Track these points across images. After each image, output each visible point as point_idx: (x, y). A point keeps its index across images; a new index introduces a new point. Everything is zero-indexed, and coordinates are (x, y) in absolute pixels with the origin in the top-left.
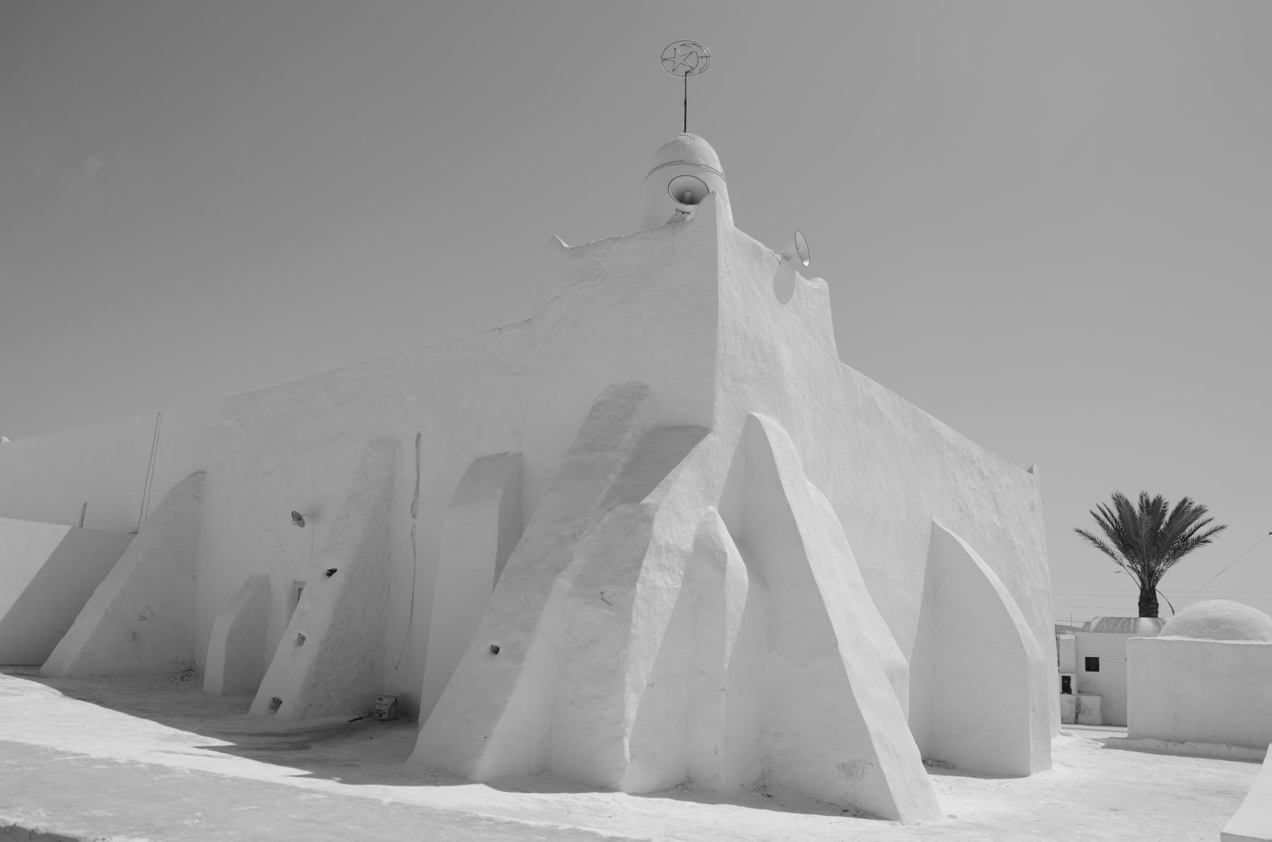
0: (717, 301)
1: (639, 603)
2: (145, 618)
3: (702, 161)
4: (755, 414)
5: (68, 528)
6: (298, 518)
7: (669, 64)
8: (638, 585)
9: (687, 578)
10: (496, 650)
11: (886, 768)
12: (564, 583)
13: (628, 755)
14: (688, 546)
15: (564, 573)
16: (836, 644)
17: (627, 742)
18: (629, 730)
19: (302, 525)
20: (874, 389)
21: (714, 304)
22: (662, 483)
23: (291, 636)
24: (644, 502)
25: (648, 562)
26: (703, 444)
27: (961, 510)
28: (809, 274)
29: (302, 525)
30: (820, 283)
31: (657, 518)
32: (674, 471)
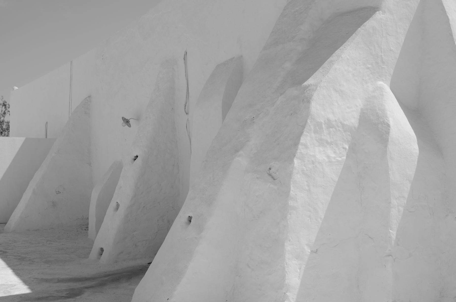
1: (297, 177)
2: (59, 192)
5: (23, 139)
6: (127, 122)
8: (296, 161)
9: (353, 150)
10: (190, 219)
12: (241, 161)
14: (353, 120)
15: (241, 152)
19: (130, 126)
22: (326, 65)
23: (113, 205)
24: (306, 83)
25: (307, 139)
26: (370, 24)
29: (130, 126)
31: (315, 96)
32: (338, 52)
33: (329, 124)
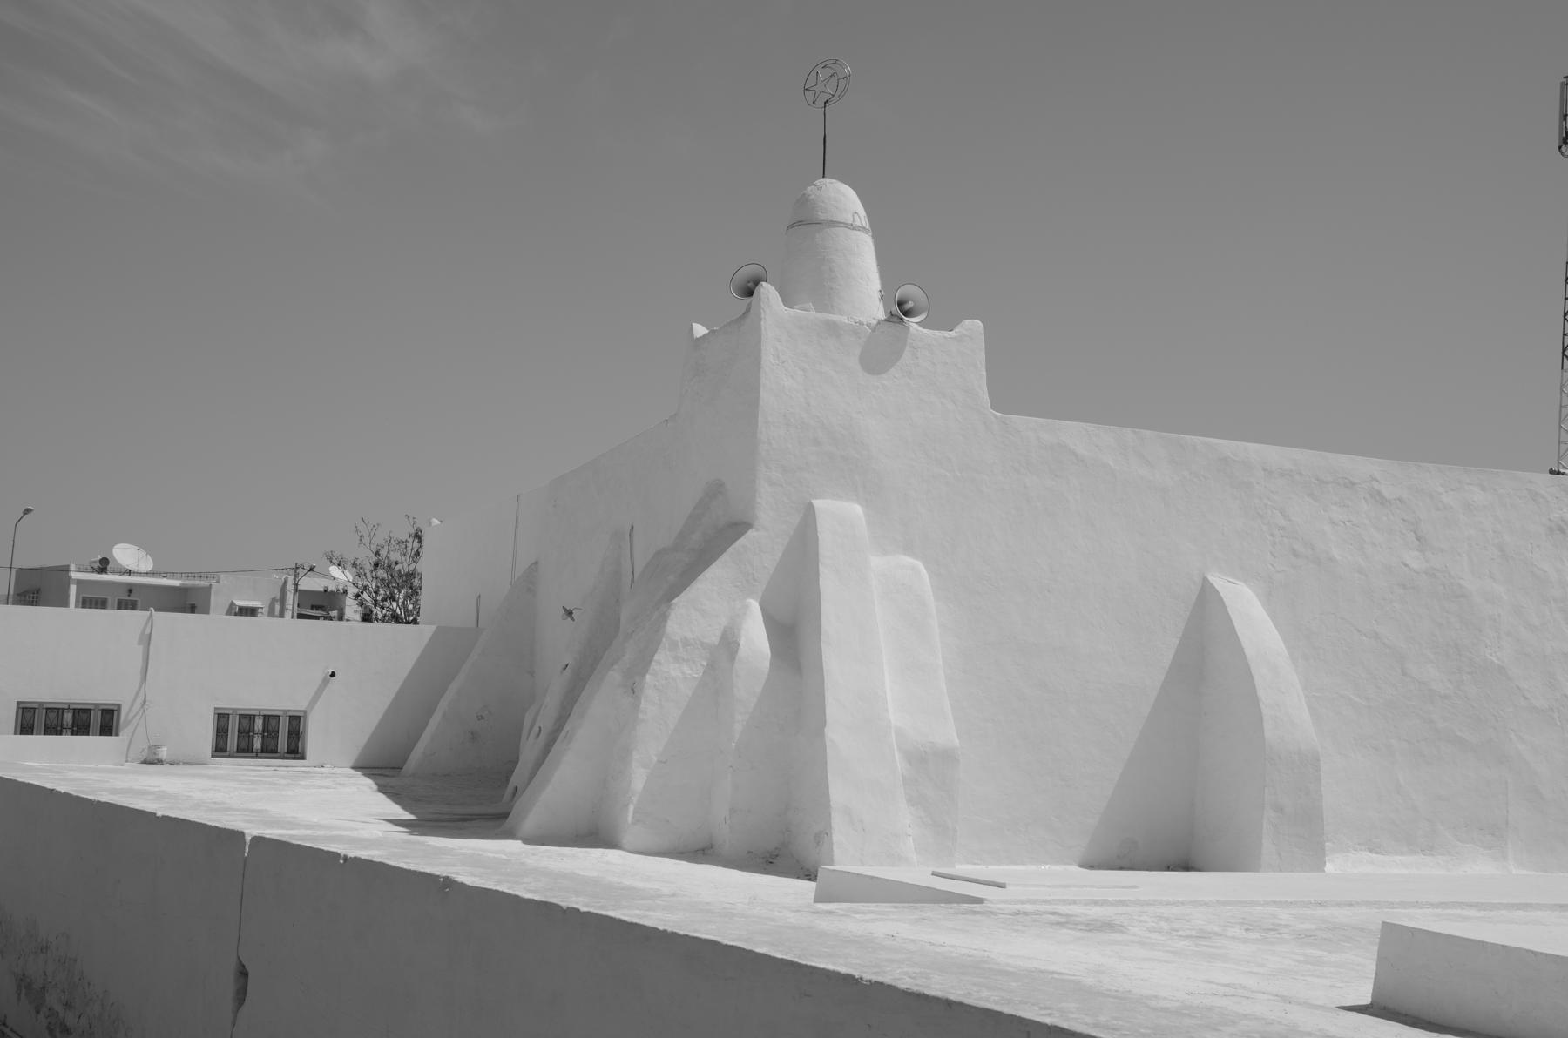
0: (757, 399)
3: (822, 217)
4: (817, 503)
5: (434, 628)
6: (569, 613)
7: (810, 95)
9: (712, 667)
11: (837, 837)
13: (630, 819)
14: (714, 639)
16: (824, 723)
17: (631, 808)
18: (635, 799)
20: (1075, 435)
21: (754, 403)
23: (536, 729)
27: (1296, 554)
28: (944, 321)
30: (973, 327)
33: (686, 643)
